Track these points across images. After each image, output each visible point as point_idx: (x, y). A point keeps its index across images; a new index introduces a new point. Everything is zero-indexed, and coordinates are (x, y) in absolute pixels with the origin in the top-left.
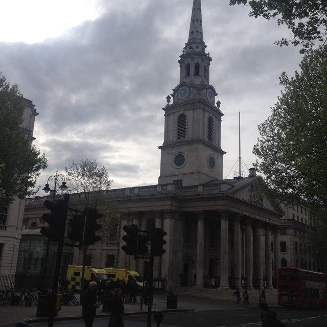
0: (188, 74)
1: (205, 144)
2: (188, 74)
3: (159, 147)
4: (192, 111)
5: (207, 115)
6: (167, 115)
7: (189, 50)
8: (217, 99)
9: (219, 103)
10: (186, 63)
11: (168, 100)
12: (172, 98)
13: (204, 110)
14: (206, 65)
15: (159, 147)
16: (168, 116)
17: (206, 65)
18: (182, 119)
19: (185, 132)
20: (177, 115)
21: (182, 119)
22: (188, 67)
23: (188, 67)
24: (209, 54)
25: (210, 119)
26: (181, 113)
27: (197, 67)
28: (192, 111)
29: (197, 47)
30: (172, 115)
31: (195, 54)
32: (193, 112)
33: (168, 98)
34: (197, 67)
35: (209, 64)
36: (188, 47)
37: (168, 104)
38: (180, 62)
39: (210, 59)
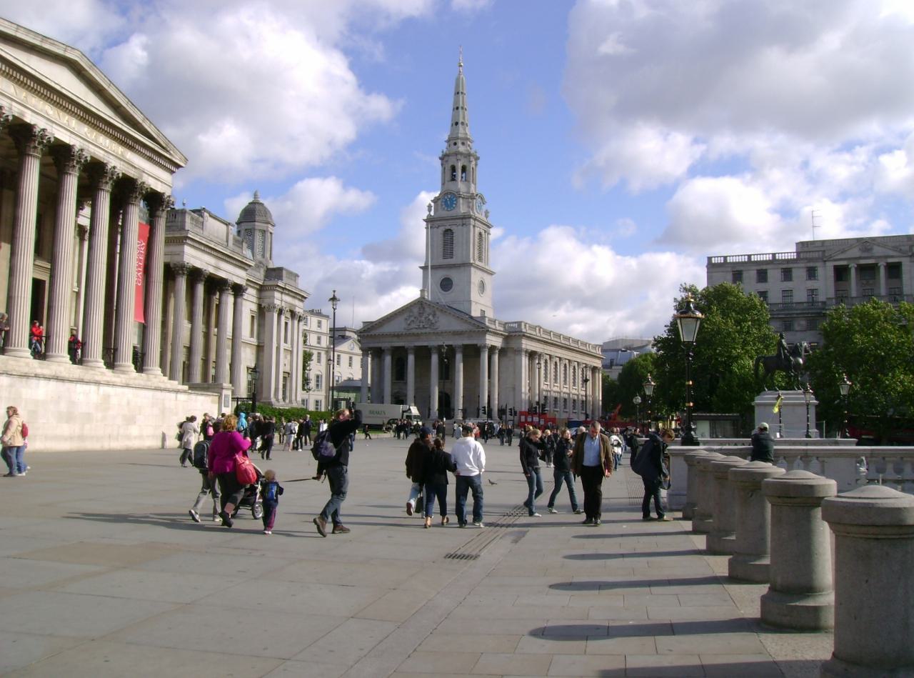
1: (477, 267)
2: (453, 178)
3: (421, 267)
4: (460, 227)
5: (477, 230)
7: (454, 149)
8: (484, 208)
9: (487, 213)
11: (430, 210)
12: (433, 204)
13: (474, 226)
14: (474, 167)
15: (421, 267)
17: (474, 167)
18: (448, 232)
19: (452, 254)
20: (442, 229)
21: (448, 232)
23: (453, 169)
24: (476, 152)
25: (480, 234)
26: (448, 227)
27: (464, 169)
29: (463, 144)
31: (461, 154)
33: (430, 206)
34: (464, 169)
35: (476, 165)
36: (452, 142)
37: (430, 215)
38: (441, 159)
39: (477, 159)
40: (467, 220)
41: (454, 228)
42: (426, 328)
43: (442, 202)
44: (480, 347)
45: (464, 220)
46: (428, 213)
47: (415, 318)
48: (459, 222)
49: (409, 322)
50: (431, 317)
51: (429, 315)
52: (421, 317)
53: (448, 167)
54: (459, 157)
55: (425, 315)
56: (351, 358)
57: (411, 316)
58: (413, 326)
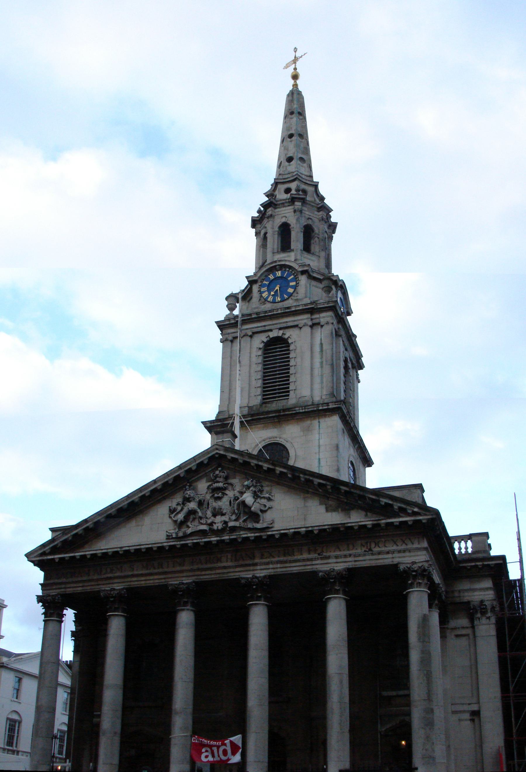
0: (285, 245)
2: (285, 245)
6: (227, 341)
10: (278, 221)
11: (231, 308)
16: (232, 341)
18: (276, 352)
22: (285, 230)
23: (285, 230)
28: (308, 330)
30: (248, 339)
32: (312, 333)
34: (308, 232)
38: (255, 223)
40: (323, 315)
41: (288, 333)
42: (234, 529)
43: (261, 286)
44: (405, 571)
45: (316, 316)
46: (228, 312)
47: (200, 504)
48: (304, 319)
49: (180, 517)
50: (248, 498)
51: (242, 493)
52: (219, 498)
53: (272, 227)
54: (298, 204)
55: (230, 494)
56: (20, 680)
57: (187, 500)
58: (193, 527)
